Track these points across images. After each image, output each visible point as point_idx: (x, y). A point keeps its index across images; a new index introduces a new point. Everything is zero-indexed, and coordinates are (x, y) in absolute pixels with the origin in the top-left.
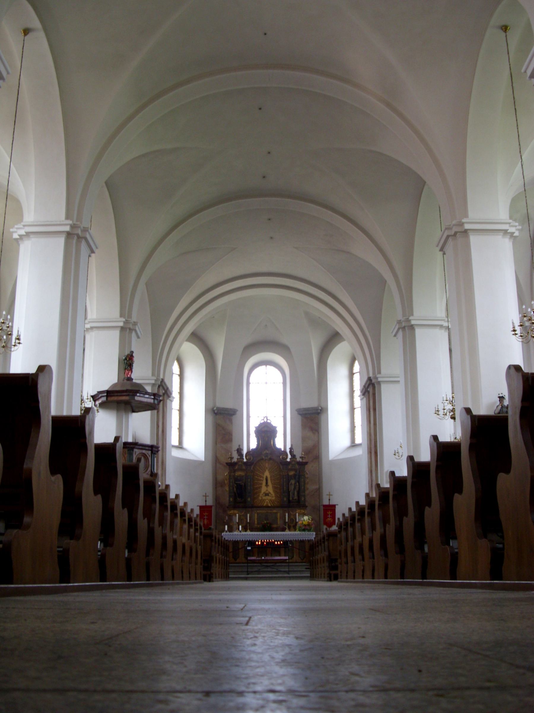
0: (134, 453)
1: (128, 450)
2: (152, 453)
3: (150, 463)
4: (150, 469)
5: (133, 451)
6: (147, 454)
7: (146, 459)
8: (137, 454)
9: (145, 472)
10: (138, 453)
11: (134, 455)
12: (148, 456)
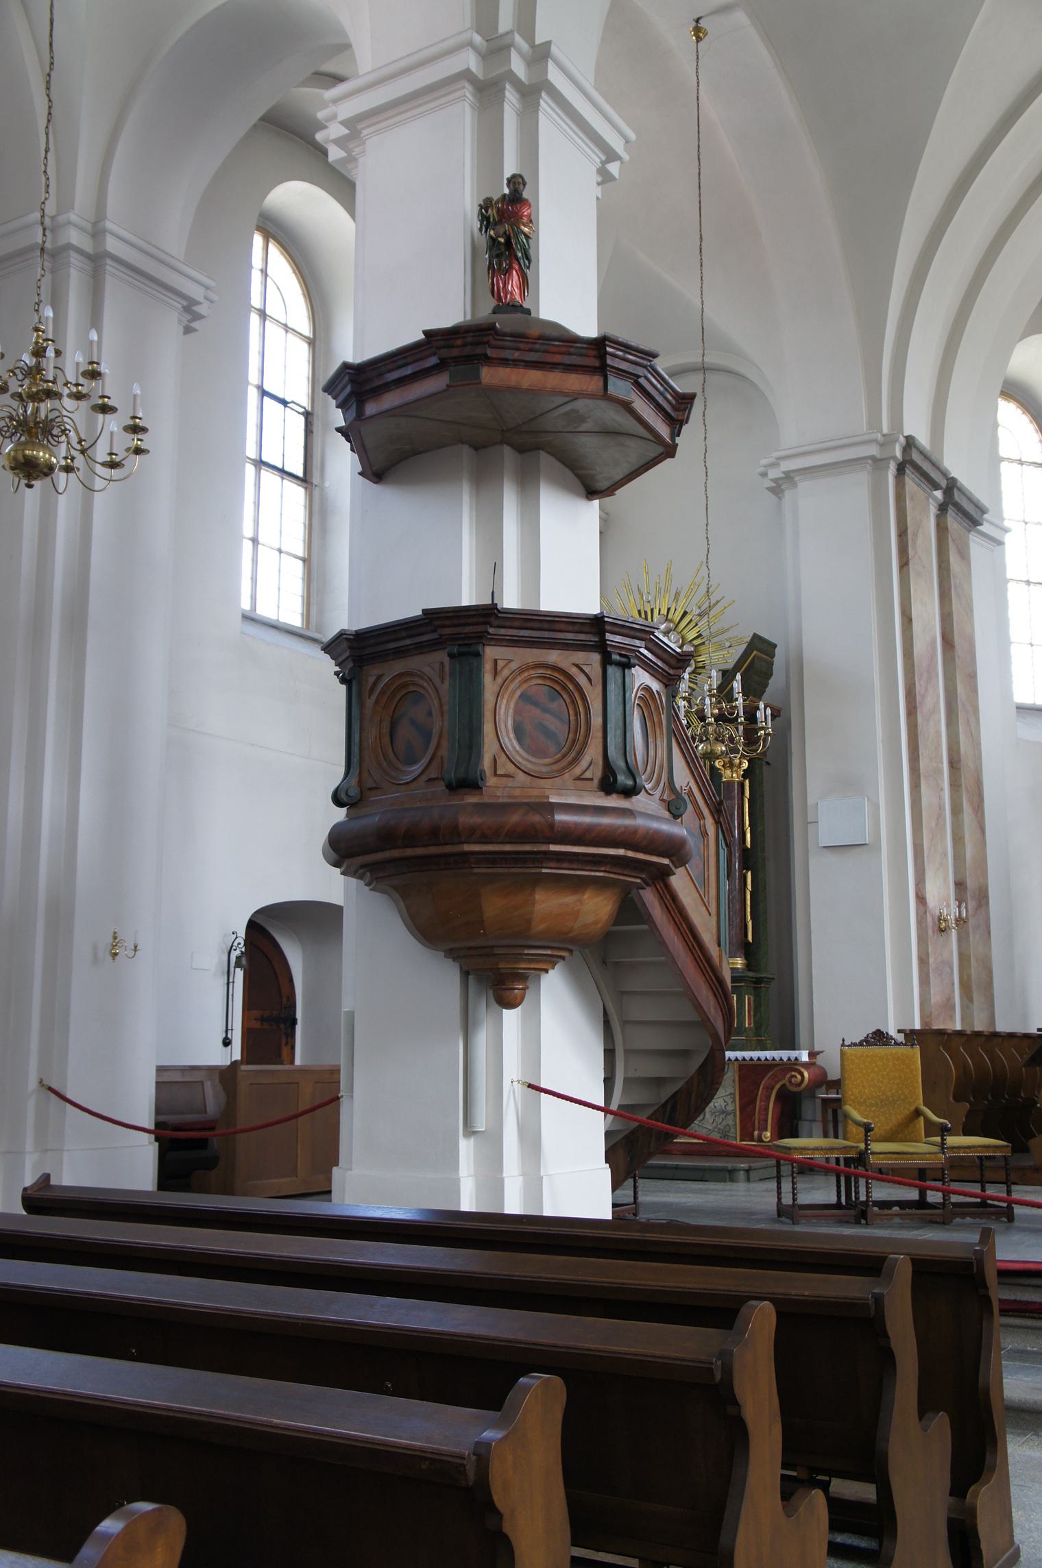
0: (488, 666)
1: (451, 656)
2: (606, 661)
3: (597, 721)
4: (593, 752)
5: (478, 655)
6: (574, 671)
7: (574, 702)
8: (506, 672)
9: (561, 772)
10: (514, 666)
11: (487, 678)
12: (582, 680)
